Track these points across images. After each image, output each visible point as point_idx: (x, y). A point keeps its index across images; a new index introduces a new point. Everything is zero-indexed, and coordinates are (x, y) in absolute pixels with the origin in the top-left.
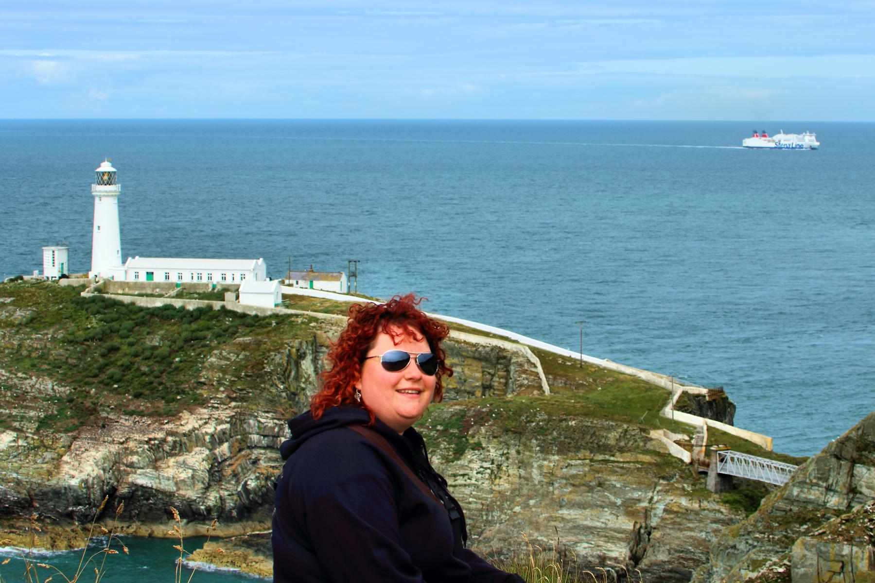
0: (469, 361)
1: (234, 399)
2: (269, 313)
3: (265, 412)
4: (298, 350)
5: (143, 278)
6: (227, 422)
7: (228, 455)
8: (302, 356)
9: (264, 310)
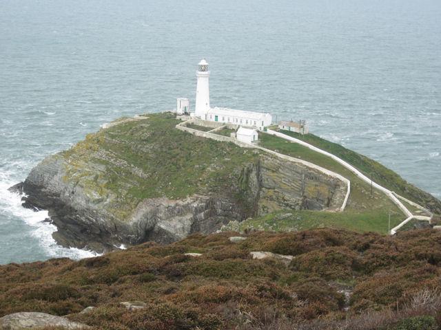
0: (323, 185)
2: (246, 146)
4: (248, 168)
7: (203, 218)
8: (249, 171)
9: (244, 144)
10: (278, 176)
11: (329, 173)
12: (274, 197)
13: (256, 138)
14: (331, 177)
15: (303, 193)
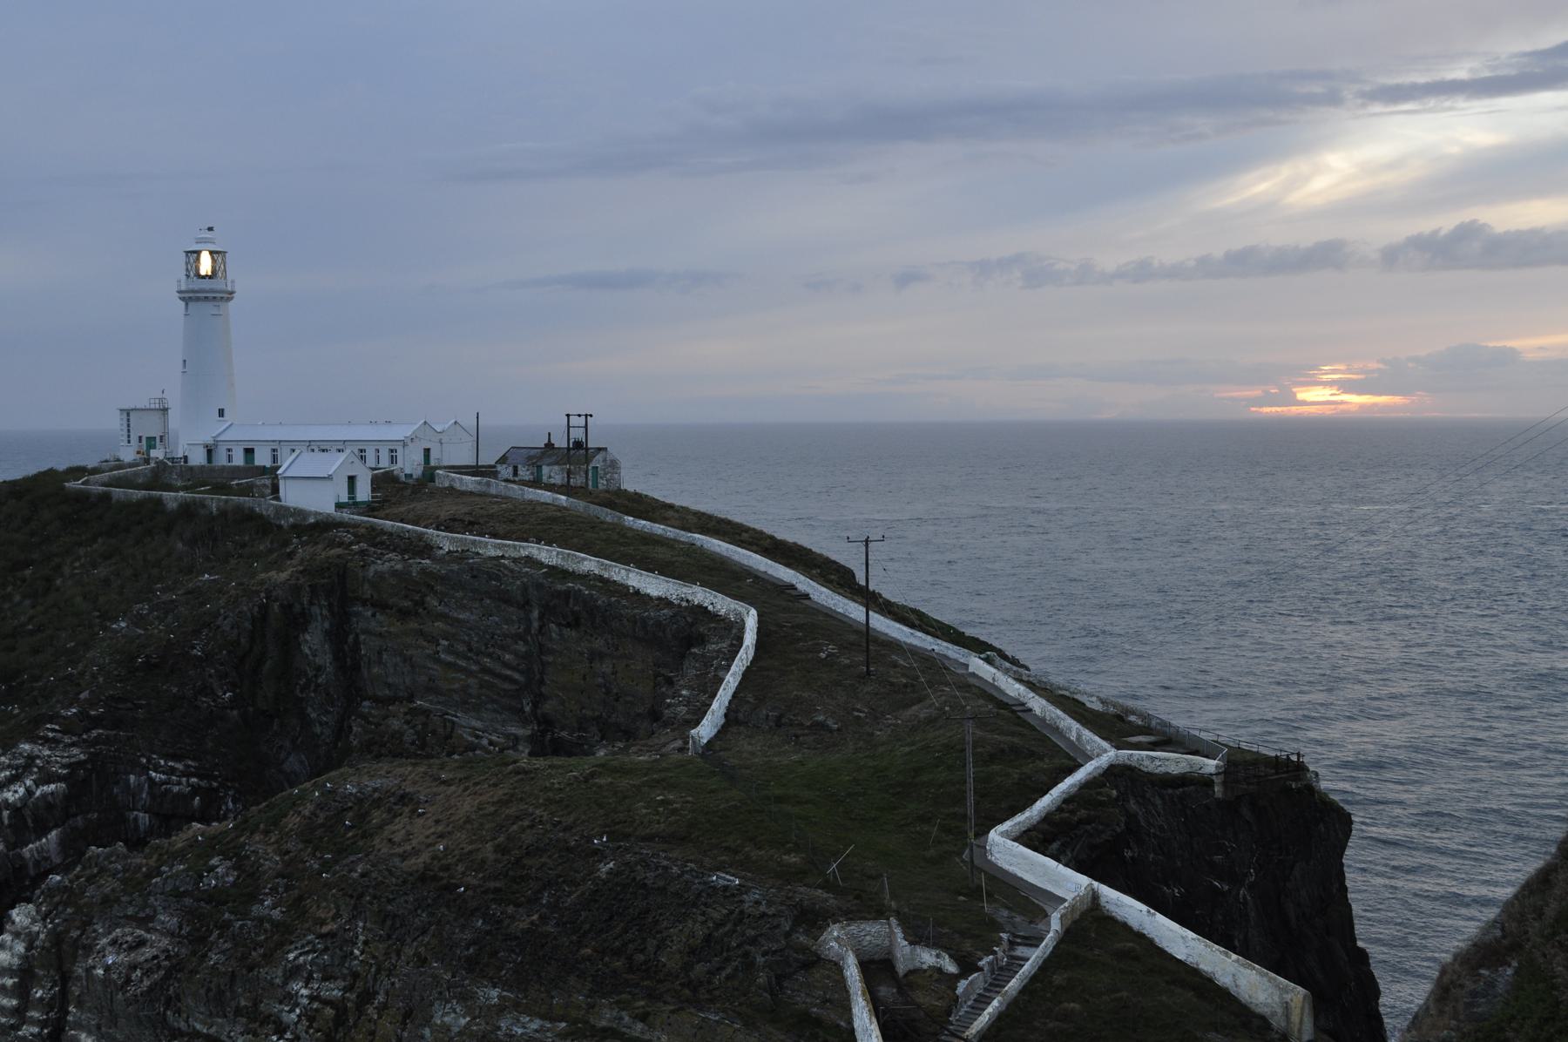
1: (97, 722)
3: (168, 757)
5: (239, 460)
6: (59, 778)
7: (57, 860)
8: (297, 621)
10: (421, 633)
11: (654, 586)
12: (409, 736)
13: (364, 493)
14: (664, 602)
15: (538, 700)
